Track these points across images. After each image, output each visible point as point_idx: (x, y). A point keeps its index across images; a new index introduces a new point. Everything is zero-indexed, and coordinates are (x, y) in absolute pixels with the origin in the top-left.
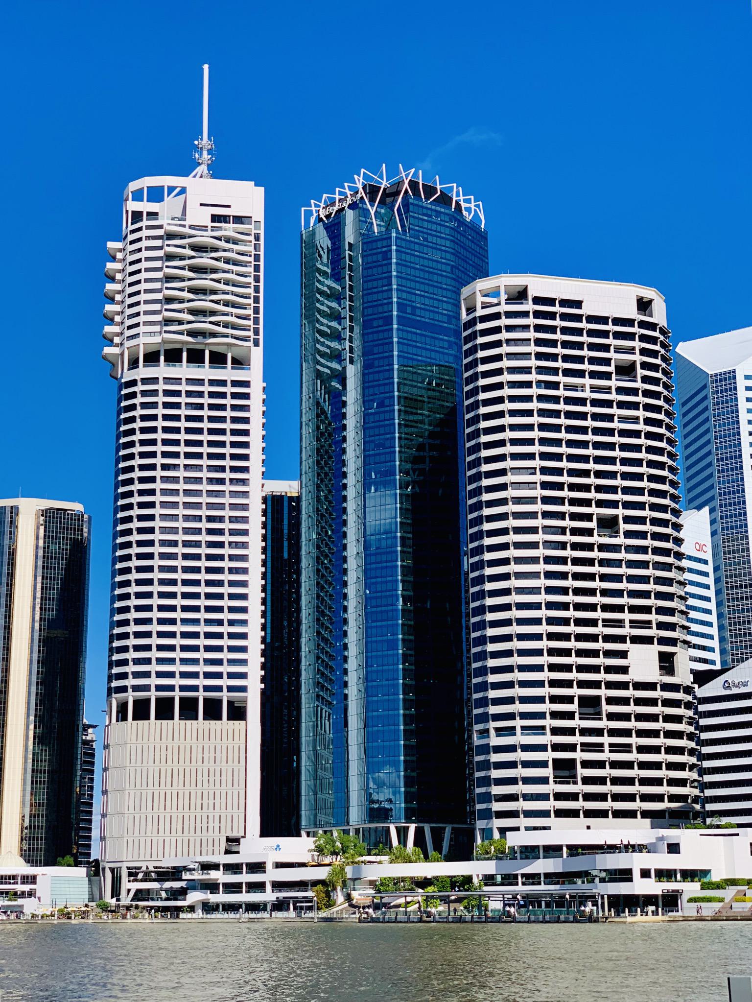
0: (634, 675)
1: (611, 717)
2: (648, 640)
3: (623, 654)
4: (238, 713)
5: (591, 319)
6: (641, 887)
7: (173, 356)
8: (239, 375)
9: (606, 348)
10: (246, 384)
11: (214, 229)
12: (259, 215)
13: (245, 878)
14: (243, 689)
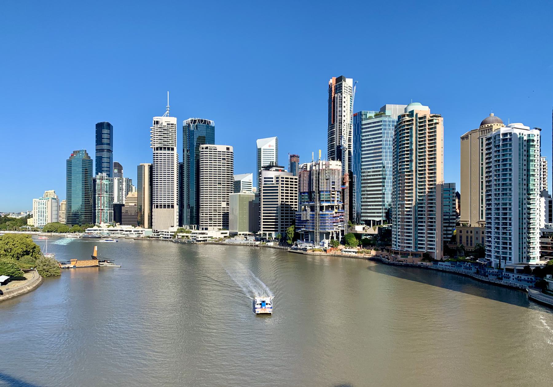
4: (173, 207)
6: (200, 239)
7: (161, 149)
8: (172, 152)
12: (175, 123)
13: (167, 234)
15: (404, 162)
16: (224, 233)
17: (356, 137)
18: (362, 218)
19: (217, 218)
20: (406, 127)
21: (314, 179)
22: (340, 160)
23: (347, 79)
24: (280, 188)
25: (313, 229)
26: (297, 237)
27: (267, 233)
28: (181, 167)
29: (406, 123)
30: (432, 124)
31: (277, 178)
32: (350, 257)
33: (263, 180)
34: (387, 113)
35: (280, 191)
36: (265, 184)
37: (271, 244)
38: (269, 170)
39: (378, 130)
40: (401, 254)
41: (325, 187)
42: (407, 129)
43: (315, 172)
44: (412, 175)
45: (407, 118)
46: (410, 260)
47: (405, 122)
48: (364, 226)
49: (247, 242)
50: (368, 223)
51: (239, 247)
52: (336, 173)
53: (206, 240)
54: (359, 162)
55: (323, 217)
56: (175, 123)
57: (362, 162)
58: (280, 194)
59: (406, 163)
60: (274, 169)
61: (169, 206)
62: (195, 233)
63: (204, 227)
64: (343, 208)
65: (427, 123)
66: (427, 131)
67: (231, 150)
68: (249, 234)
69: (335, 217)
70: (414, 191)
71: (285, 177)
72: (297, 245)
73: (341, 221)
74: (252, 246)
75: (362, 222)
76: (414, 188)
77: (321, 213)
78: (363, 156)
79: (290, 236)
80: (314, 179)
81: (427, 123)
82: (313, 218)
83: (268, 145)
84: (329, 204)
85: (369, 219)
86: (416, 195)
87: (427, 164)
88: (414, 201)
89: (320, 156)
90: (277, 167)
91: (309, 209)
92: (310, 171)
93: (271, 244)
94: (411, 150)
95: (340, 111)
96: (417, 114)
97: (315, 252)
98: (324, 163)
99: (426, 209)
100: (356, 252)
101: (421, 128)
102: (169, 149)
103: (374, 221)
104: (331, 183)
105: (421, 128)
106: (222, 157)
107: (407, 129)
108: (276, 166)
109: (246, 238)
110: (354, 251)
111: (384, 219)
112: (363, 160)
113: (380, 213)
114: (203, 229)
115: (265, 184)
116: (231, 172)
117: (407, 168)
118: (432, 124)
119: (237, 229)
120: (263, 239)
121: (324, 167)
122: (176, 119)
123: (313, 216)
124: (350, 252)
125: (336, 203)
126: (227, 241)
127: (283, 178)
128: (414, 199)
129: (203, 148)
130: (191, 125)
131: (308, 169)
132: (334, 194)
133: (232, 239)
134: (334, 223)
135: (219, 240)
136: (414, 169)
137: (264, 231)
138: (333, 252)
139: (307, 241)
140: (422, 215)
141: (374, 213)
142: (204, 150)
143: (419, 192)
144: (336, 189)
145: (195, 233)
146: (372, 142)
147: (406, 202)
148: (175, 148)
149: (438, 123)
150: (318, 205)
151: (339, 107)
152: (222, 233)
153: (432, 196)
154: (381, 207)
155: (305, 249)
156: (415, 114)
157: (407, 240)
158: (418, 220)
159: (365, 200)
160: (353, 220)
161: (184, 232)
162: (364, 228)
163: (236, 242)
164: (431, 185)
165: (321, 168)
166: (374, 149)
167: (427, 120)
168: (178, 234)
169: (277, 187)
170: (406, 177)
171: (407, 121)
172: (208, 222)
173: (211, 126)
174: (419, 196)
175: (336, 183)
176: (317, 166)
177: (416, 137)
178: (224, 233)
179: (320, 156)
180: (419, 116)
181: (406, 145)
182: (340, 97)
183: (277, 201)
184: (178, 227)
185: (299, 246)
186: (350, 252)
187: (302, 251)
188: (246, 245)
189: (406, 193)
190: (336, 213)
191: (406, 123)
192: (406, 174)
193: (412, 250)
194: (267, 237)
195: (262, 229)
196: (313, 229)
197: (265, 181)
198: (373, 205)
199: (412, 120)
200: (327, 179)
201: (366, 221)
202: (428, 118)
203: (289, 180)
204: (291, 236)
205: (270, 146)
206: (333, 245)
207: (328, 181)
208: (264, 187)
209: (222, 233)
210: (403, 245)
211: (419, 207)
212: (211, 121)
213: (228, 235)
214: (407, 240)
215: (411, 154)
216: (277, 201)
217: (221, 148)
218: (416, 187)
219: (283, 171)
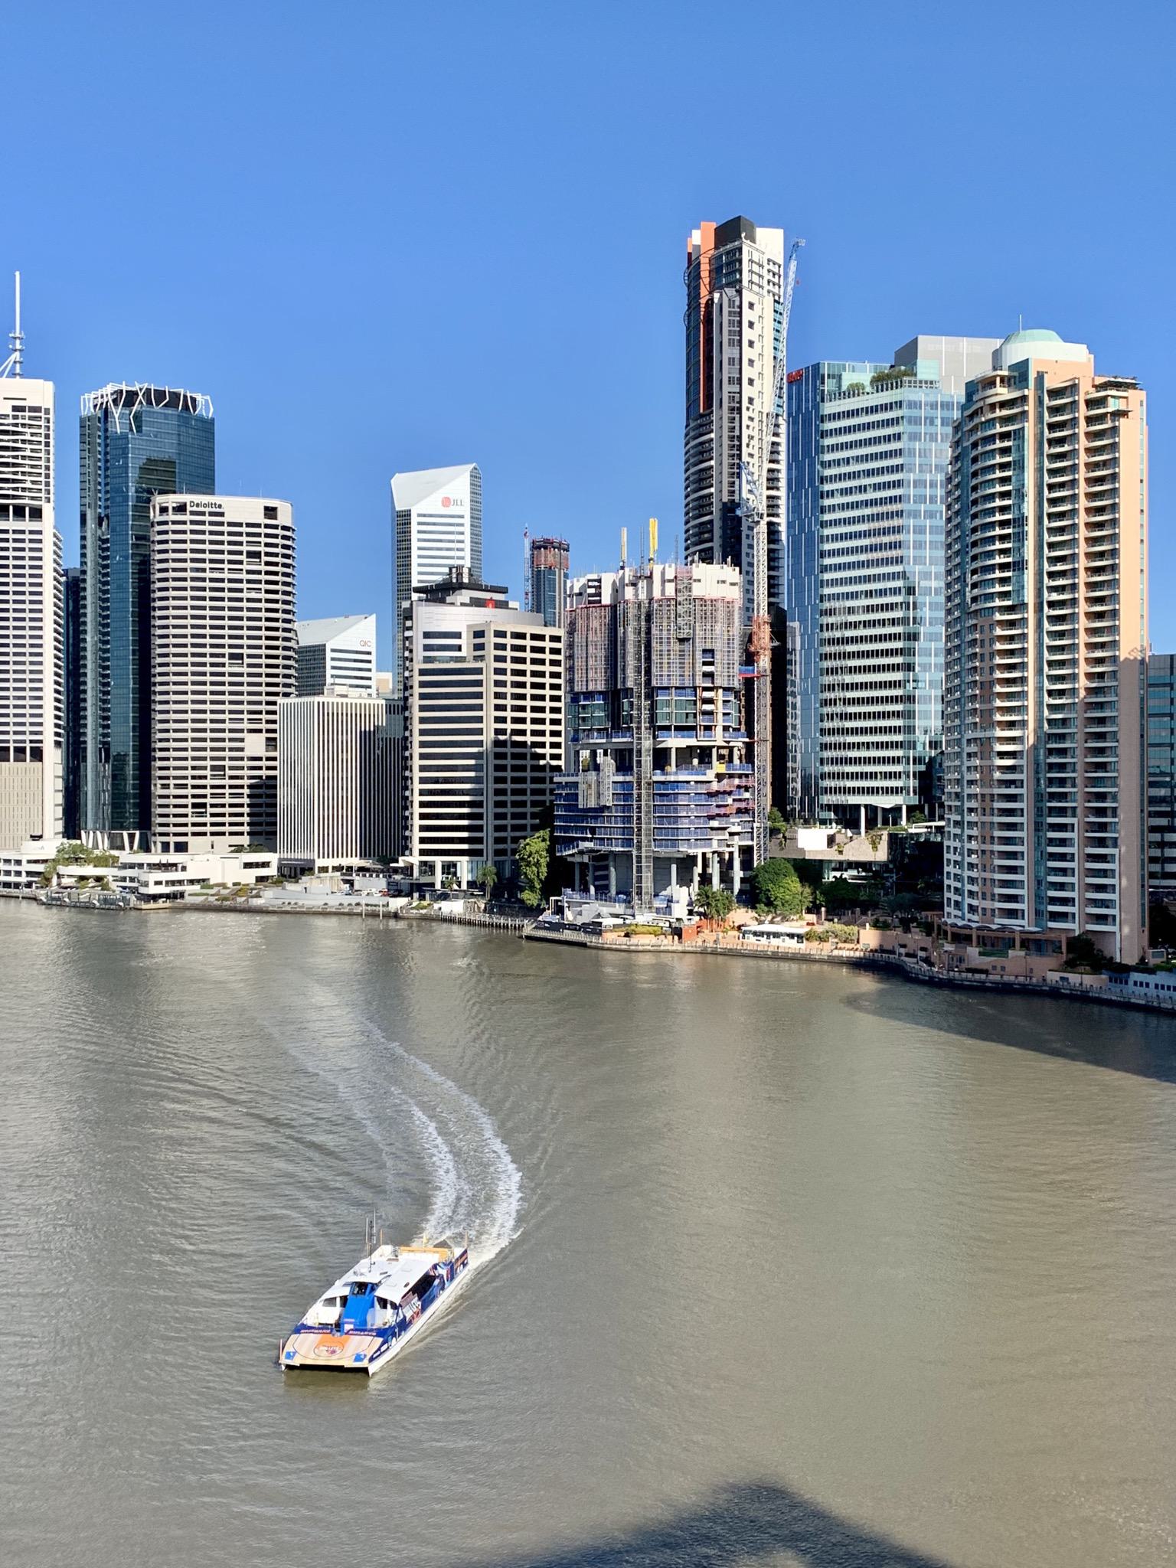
0: (246, 754)
1: (232, 778)
2: (260, 731)
3: (242, 740)
5: (230, 524)
8: (35, 526)
9: (241, 544)
10: (40, 532)
11: (15, 417)
12: (48, 402)
14: (41, 741)
15: (991, 568)
16: (257, 865)
17: (800, 469)
18: (826, 799)
19: (227, 800)
20: (999, 429)
21: (631, 637)
22: (737, 562)
23: (760, 232)
24: (489, 678)
25: (628, 842)
26: (561, 876)
27: (438, 861)
28: (73, 588)
29: (999, 413)
30: (1101, 418)
31: (479, 634)
32: (776, 957)
33: (419, 642)
34: (925, 369)
35: (489, 689)
36: (427, 660)
37: (454, 907)
38: (442, 601)
39: (888, 439)
40: (982, 941)
41: (676, 671)
42: (1004, 436)
43: (632, 612)
44: (1023, 622)
45: (1003, 393)
46: (1015, 964)
47: (993, 406)
48: (834, 829)
49: (353, 899)
50: (848, 817)
51: (319, 922)
52: (720, 615)
53: (182, 895)
54: (809, 572)
55: (666, 793)
56: (48, 402)
57: (825, 569)
58: (489, 702)
59: (998, 574)
60: (465, 596)
61: (20, 751)
62: (132, 866)
63: (172, 840)
64: (749, 756)
65: (1083, 412)
66: (1083, 443)
67: (284, 517)
68: (361, 869)
69: (717, 793)
70: (1031, 688)
71: (510, 629)
72: (559, 910)
73: (739, 811)
74: (374, 915)
75: (824, 815)
76: (1030, 673)
77: (659, 777)
78: (827, 547)
79: (531, 872)
80: (631, 637)
81: (1083, 412)
82: (627, 797)
83: (439, 499)
84: (693, 742)
85: (853, 800)
86: (1039, 703)
87: (1082, 578)
88: (1031, 725)
89: (654, 543)
90: (479, 588)
91: (607, 763)
92: (613, 608)
93: (454, 907)
94: (1020, 521)
95: (731, 361)
96: (1040, 377)
97: (634, 940)
98: (670, 575)
99: (1079, 759)
100: (800, 937)
101: (1059, 434)
102: (19, 512)
103: (871, 809)
104: (699, 655)
105: (1059, 434)
106: (245, 548)
107: (1004, 436)
108: (474, 586)
109: (351, 883)
110: (792, 931)
111: (914, 800)
112: (827, 561)
113: (896, 775)
114: (166, 847)
115: (427, 660)
116: (282, 612)
117: (1005, 595)
118: (1101, 418)
119: (309, 846)
120: (421, 889)
121: (670, 590)
122: (49, 386)
123: (625, 794)
124: (776, 935)
125: (718, 738)
126: (269, 897)
127: (500, 634)
128: (1031, 718)
129: (164, 510)
130: (116, 412)
131: (606, 599)
132: (710, 701)
133: (290, 887)
134: (711, 818)
135: (237, 894)
136: (1029, 597)
137: (423, 852)
138: (709, 937)
139: (603, 891)
140: (1062, 782)
141: (873, 776)
142: (171, 516)
143: (1050, 693)
144: (718, 682)
145: (132, 866)
146: (862, 489)
147: (999, 733)
148: (48, 511)
149: (1124, 414)
150: (647, 744)
151: (731, 343)
152: (248, 865)
153: (1101, 706)
154: (899, 753)
155: (595, 928)
156: (1032, 376)
157: (1005, 884)
158: (1050, 803)
159: (836, 724)
160: (789, 805)
161: (87, 861)
162: (831, 840)
163: (314, 902)
164: (1100, 661)
165: (657, 594)
166: (873, 518)
167: (1081, 399)
168: (62, 869)
169: (479, 671)
170: (999, 632)
171: (1003, 405)
172: (190, 820)
173: (201, 420)
174: (1053, 708)
175: (718, 656)
176: (642, 584)
177: (1040, 469)
178: (257, 865)
179: (654, 543)
180: (1050, 383)
181: (998, 503)
182: (731, 303)
183: (480, 732)
184: (61, 841)
185: (569, 915)
186: (776, 935)
187: (581, 937)
188: (350, 914)
189: (1000, 695)
190: (720, 777)
191: (999, 413)
192: (998, 617)
193: (1025, 924)
194: (439, 877)
195: (417, 846)
196: (628, 842)
197: (427, 648)
198: (867, 746)
199: (1024, 399)
200: (682, 641)
201: (837, 808)
202: (1086, 391)
203: (529, 643)
204: (538, 870)
205: (446, 502)
206: (708, 908)
207: (687, 646)
208: (422, 672)
209: (248, 865)
210: (988, 904)
211: (1051, 752)
212: (199, 397)
213: (272, 871)
214: (1005, 884)
215: (1020, 537)
216: (480, 732)
217: (242, 509)
218: (1039, 671)
219: (503, 605)
